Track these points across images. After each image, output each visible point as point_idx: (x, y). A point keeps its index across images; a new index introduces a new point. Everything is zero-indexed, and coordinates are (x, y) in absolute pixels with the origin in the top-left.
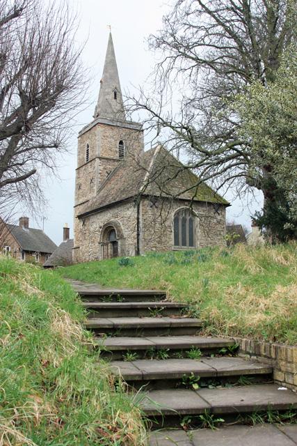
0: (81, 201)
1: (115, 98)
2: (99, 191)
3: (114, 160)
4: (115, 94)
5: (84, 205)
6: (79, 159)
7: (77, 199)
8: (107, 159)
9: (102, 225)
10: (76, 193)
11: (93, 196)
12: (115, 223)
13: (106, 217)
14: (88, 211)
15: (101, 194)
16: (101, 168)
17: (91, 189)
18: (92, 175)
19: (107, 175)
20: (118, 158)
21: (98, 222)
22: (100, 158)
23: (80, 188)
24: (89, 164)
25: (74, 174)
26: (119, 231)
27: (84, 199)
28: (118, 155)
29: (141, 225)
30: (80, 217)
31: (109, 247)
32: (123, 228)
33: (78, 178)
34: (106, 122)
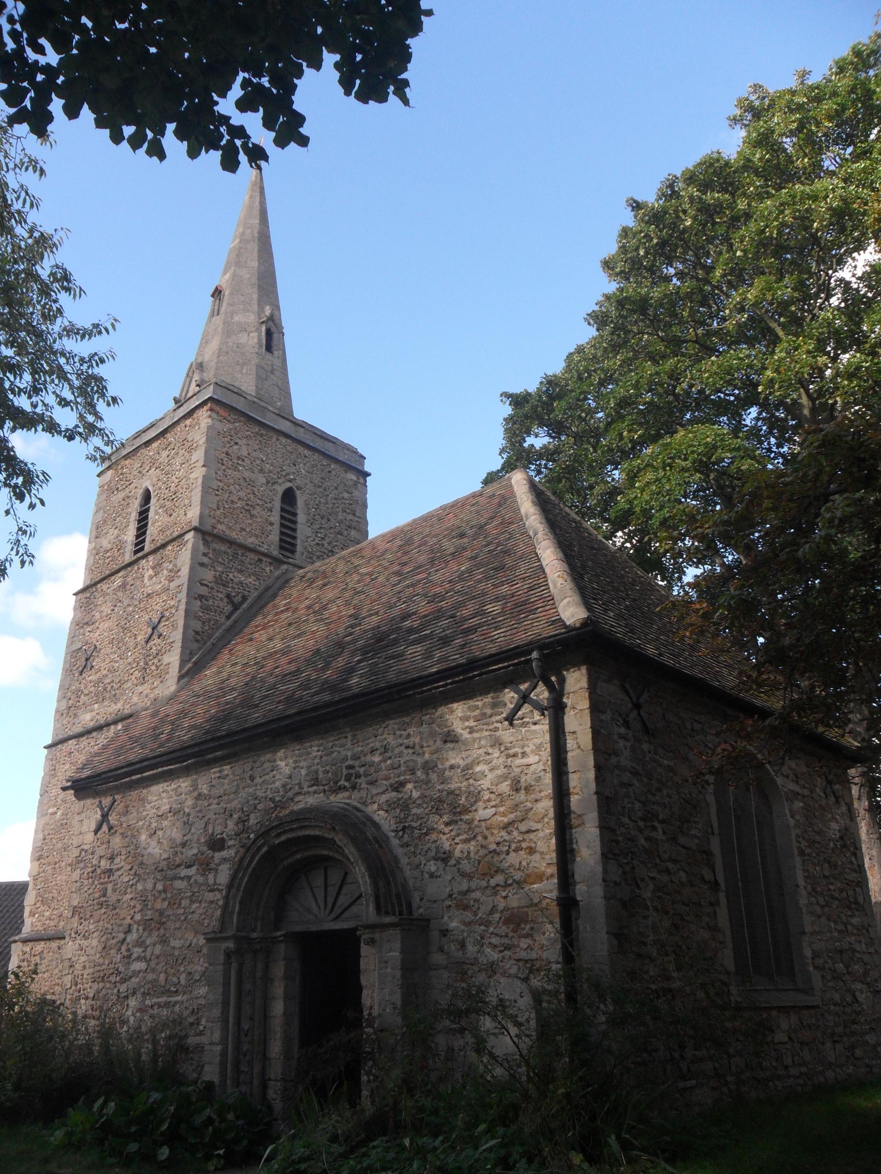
0: (87, 719)
2: (192, 668)
5: (102, 738)
8: (231, 543)
10: (65, 690)
14: (132, 757)
15: (210, 677)
16: (208, 575)
17: (147, 668)
18: (157, 605)
19: (228, 608)
20: (276, 553)
24: (147, 564)
25: (71, 601)
27: (112, 709)
28: (274, 537)
30: (83, 787)
31: (279, 969)
32: (399, 852)
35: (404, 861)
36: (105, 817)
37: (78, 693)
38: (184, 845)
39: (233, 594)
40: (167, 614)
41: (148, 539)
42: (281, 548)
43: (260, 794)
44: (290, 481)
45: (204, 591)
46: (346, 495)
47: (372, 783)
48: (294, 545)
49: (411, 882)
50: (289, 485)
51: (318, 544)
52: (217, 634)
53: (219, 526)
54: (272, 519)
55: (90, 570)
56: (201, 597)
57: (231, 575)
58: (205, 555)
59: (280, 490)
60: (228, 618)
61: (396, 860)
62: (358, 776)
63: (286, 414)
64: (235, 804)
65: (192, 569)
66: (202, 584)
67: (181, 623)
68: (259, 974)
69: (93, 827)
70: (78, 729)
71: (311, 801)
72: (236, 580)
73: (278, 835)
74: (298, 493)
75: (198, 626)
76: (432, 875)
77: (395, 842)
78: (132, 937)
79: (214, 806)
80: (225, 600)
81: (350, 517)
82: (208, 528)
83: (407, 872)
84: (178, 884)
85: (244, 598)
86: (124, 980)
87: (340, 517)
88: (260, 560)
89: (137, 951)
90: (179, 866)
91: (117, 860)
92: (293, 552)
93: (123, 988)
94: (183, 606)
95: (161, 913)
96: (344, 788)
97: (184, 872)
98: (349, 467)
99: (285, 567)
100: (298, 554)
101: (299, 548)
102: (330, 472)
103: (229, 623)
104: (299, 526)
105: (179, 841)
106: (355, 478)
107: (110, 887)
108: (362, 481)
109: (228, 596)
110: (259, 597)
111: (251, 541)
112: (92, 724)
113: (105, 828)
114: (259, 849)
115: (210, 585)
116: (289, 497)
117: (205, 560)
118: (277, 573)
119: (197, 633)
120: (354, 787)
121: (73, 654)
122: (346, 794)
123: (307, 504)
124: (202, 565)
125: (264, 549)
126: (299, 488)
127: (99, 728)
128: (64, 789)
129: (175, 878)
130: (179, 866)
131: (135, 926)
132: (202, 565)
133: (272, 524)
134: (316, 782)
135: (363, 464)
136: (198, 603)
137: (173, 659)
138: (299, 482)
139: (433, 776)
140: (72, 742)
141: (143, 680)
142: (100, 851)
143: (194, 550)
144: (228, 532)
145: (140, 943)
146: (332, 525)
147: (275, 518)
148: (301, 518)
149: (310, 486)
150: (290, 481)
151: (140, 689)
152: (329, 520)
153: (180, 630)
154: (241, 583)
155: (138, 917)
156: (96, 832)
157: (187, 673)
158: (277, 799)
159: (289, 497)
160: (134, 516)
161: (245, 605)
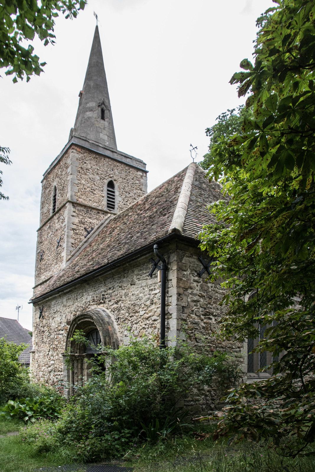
1: (103, 118)
3: (99, 211)
4: (103, 111)
6: (42, 214)
7: (38, 276)
9: (71, 317)
10: (37, 267)
11: (60, 269)
12: (98, 313)
13: (84, 302)
16: (76, 220)
19: (85, 233)
20: (105, 209)
21: (64, 313)
22: (75, 204)
23: (41, 259)
25: (36, 234)
26: (109, 335)
28: (105, 202)
29: (173, 323)
33: (40, 243)
34: (86, 145)
35: (117, 330)
36: (41, 313)
37: (40, 269)
38: (61, 323)
39: (87, 227)
40: (62, 237)
41: (56, 207)
42: (108, 207)
43: (79, 305)
44: (111, 177)
45: (74, 227)
46: (137, 182)
47: (110, 301)
48: (114, 205)
49: (120, 338)
50: (110, 179)
51: (124, 204)
52: (81, 244)
53: (80, 200)
54: (103, 195)
55: (41, 221)
56: (73, 229)
57: (86, 220)
58: (74, 212)
59: (106, 182)
60: (85, 237)
61: (115, 330)
62: (106, 299)
63: (117, 150)
64: (72, 309)
65: (69, 218)
66: (73, 224)
67: (66, 240)
68: (79, 367)
69: (39, 316)
70: (41, 282)
71: (93, 307)
72: (88, 221)
73: (79, 320)
74: (115, 182)
75: (73, 241)
76: (126, 336)
77: (115, 324)
78: (50, 353)
79: (68, 309)
80: (84, 230)
81: (139, 191)
82: (75, 201)
83: (119, 335)
84: (60, 336)
85: (92, 229)
86: (50, 367)
87: (135, 192)
88: (99, 213)
89: (52, 358)
90: (60, 330)
91: (45, 328)
92: (113, 208)
93: (49, 369)
94: (66, 234)
95: (56, 345)
96: (101, 303)
97: (61, 332)
98: (138, 170)
99: (109, 215)
100: (116, 209)
101: (116, 207)
102: (129, 172)
103: (86, 239)
104: (116, 198)
105: (59, 321)
106: (141, 174)
107: (44, 336)
108: (144, 175)
109: (85, 228)
110: (98, 228)
111: (94, 205)
112: (44, 280)
113: (42, 317)
114: (74, 325)
115: (77, 224)
116: (111, 185)
117: (74, 214)
118: (106, 217)
119: (73, 244)
120: (104, 303)
121: (38, 254)
122: (102, 305)
123: (119, 187)
124: (73, 216)
125: (100, 208)
126: (115, 180)
127: (46, 281)
128: (29, 303)
129: (59, 334)
130: (60, 330)
131: (51, 350)
132: (73, 216)
133: (103, 197)
134: (94, 301)
135: (145, 168)
136: (72, 231)
137: (64, 254)
138: (115, 178)
139: (127, 298)
140: (39, 286)
141: (57, 263)
142: (41, 325)
143: (70, 210)
144: (83, 202)
145: (52, 355)
146: (131, 195)
147: (105, 194)
148: (117, 193)
149: (121, 179)
150: (111, 177)
151: (56, 266)
152: (129, 193)
153: (66, 243)
154: (90, 223)
155: (51, 347)
156: (40, 318)
157: (69, 259)
158: (84, 307)
159: (111, 185)
160: (52, 198)
161: (93, 232)
